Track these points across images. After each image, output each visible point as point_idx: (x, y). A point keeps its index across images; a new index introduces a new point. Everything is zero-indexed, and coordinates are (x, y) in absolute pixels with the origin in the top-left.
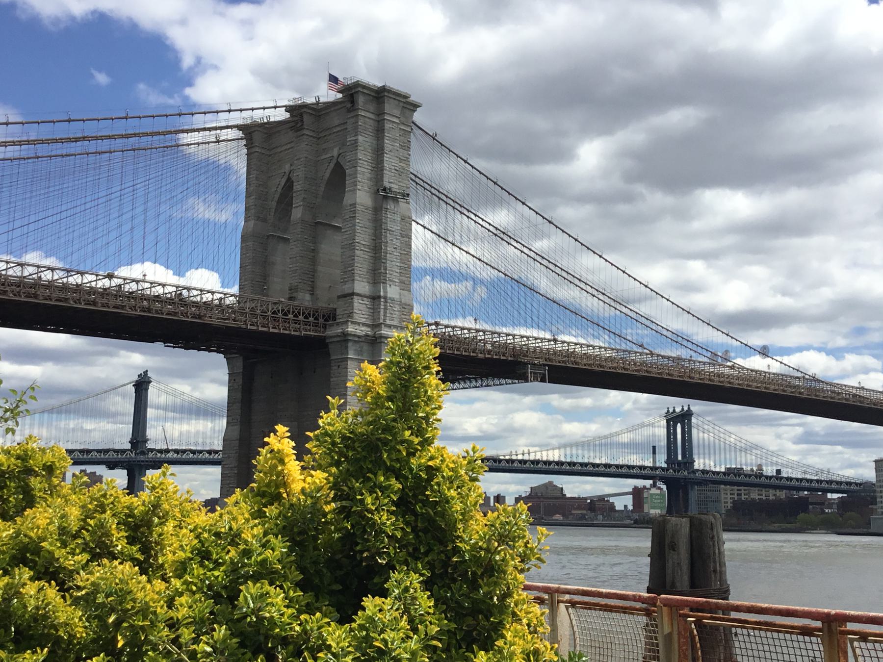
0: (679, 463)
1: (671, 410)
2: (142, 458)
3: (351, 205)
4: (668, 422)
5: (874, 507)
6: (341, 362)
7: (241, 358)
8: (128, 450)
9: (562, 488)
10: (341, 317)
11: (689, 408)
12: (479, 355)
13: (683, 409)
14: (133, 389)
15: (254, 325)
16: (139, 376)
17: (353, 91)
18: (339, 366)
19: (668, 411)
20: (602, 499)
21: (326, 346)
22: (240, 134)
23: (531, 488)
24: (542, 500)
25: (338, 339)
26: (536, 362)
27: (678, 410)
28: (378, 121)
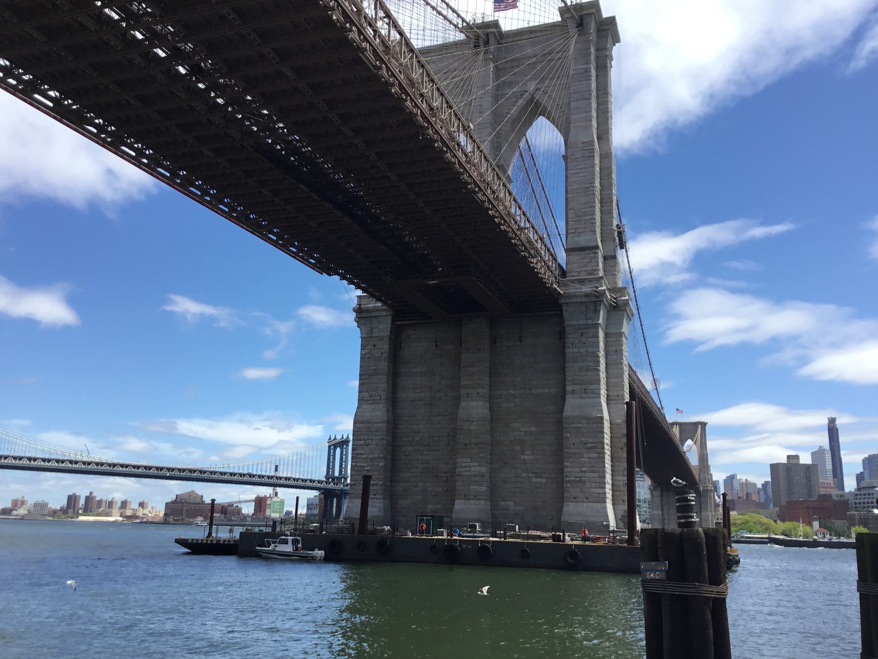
1: (333, 438)
3: (584, 143)
4: (329, 447)
6: (587, 328)
7: (389, 319)
9: (202, 496)
10: (576, 274)
11: (348, 437)
13: (343, 437)
17: (585, 12)
18: (582, 334)
20: (231, 505)
21: (559, 307)
23: (177, 496)
24: (185, 505)
25: (584, 300)
27: (339, 437)
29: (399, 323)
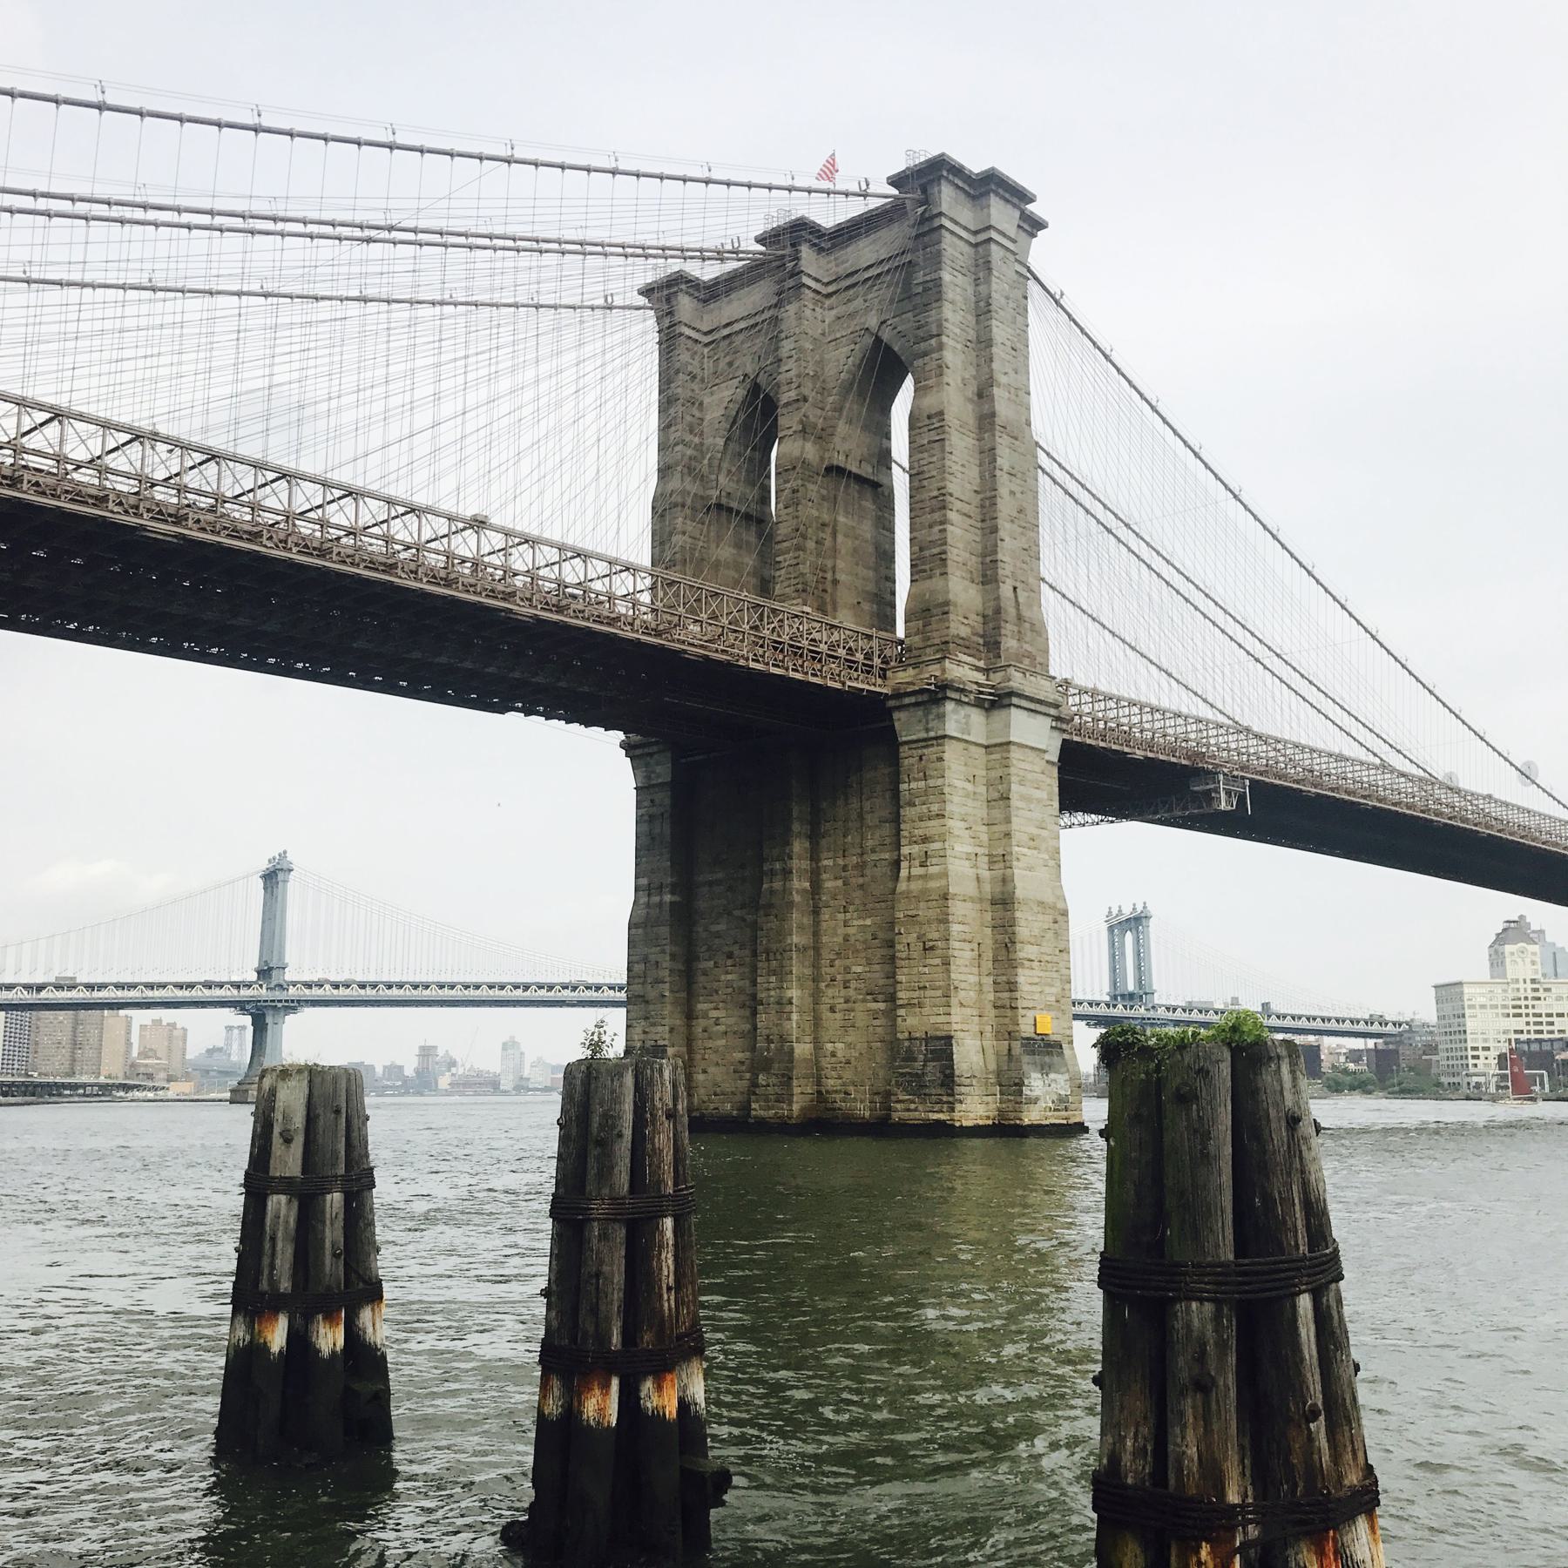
0: (1131, 996)
1: (1115, 912)
2: (278, 995)
3: (929, 417)
4: (1111, 929)
5: (1434, 1058)
7: (669, 754)
8: (255, 983)
11: (1145, 907)
12: (1138, 752)
14: (261, 883)
15: (758, 661)
16: (270, 861)
18: (921, 759)
19: (1110, 912)
22: (642, 301)
26: (1226, 770)
27: (1127, 912)
28: (976, 245)
29: (684, 761)
